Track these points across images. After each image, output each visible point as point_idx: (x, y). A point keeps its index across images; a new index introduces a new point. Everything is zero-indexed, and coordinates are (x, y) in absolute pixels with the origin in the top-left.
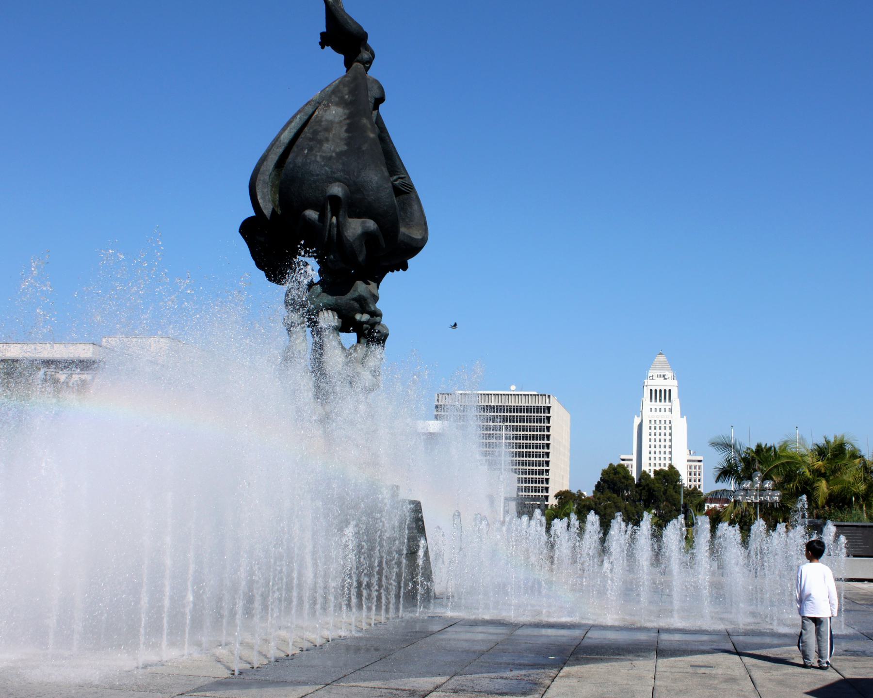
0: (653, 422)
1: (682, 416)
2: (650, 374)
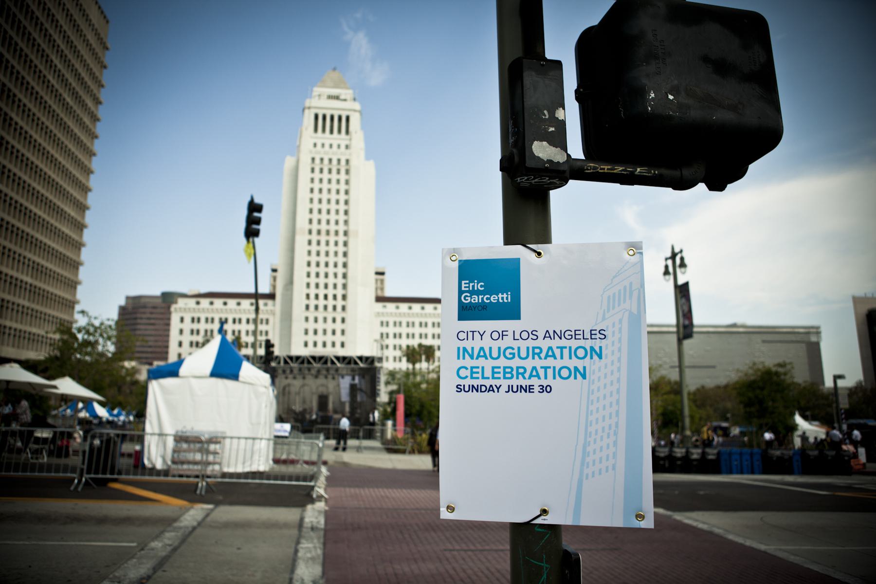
0: (317, 161)
1: (368, 158)
2: (315, 94)
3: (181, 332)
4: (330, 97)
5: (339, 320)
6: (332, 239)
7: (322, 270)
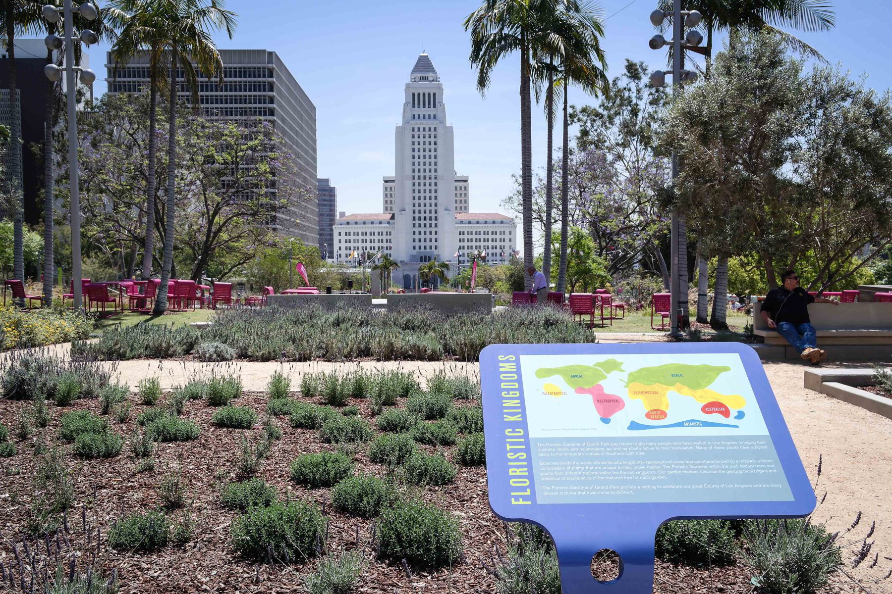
3: (340, 240)
4: (422, 79)
5: (433, 233)
6: (427, 181)
7: (422, 201)
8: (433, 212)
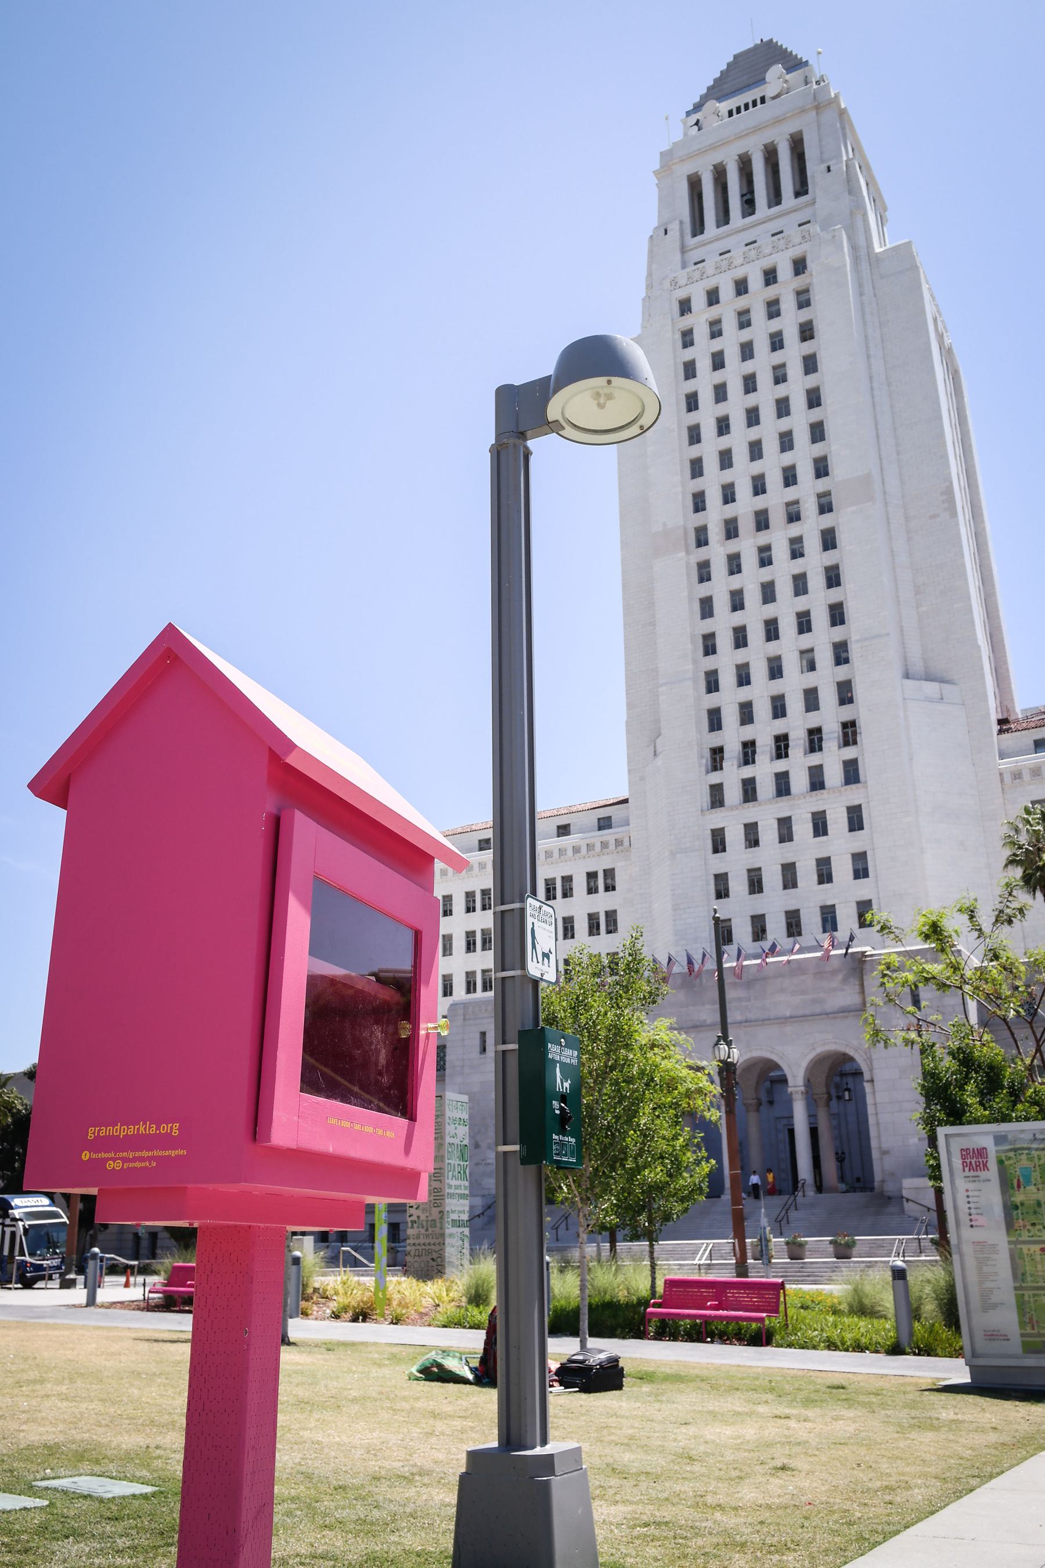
8: (828, 697)
